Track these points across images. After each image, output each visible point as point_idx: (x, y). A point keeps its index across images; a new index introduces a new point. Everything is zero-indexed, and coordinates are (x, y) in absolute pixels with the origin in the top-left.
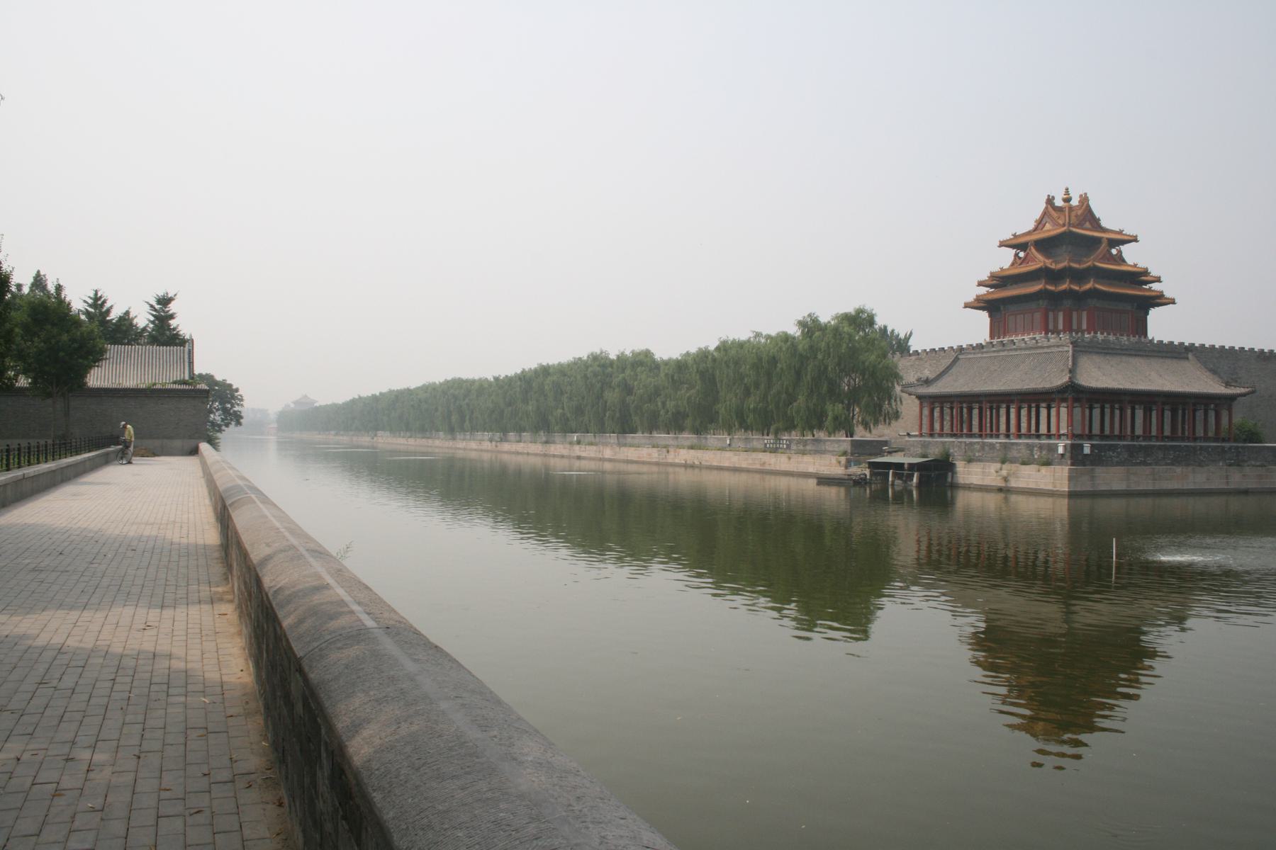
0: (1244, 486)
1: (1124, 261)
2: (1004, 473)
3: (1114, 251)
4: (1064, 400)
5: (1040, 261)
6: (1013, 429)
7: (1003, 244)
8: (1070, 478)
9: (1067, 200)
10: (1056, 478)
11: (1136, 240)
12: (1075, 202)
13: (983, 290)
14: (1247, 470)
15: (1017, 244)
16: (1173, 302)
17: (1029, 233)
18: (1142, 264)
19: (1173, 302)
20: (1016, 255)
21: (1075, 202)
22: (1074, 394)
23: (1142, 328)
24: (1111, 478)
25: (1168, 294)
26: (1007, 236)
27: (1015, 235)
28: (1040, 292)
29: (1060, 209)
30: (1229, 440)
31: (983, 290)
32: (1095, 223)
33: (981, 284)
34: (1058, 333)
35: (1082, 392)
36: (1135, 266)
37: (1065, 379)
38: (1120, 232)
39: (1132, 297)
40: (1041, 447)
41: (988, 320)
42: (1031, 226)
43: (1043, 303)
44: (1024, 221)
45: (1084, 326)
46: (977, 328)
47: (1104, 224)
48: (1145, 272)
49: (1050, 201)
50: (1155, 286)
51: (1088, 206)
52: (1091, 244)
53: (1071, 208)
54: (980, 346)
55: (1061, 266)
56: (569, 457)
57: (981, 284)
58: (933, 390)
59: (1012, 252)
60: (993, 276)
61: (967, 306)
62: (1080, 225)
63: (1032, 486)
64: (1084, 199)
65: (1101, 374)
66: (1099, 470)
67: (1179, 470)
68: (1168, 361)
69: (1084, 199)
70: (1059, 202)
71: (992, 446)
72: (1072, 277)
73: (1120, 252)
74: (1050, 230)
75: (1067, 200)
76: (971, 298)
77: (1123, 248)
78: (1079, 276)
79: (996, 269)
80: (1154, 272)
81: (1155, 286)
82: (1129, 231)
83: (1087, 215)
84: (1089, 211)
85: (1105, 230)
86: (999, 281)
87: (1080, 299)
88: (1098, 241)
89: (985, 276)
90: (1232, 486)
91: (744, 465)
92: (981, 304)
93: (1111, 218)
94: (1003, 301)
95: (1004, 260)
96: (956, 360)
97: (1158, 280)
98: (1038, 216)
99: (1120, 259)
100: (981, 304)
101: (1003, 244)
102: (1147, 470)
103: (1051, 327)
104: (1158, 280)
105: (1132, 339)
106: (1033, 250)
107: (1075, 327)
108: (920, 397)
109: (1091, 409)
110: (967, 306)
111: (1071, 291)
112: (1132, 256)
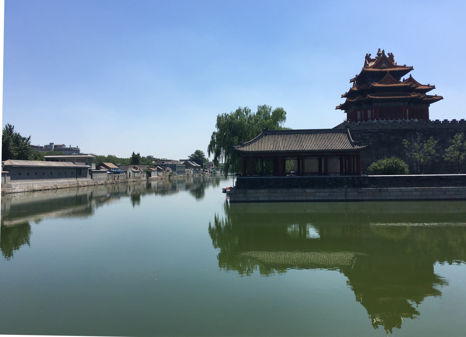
0: (360, 198)
11: (411, 69)
16: (441, 98)
19: (441, 98)
23: (426, 113)
38: (405, 66)
39: (419, 98)
66: (250, 191)
73: (410, 75)
97: (433, 87)
99: (411, 79)
104: (433, 87)
105: (390, 121)
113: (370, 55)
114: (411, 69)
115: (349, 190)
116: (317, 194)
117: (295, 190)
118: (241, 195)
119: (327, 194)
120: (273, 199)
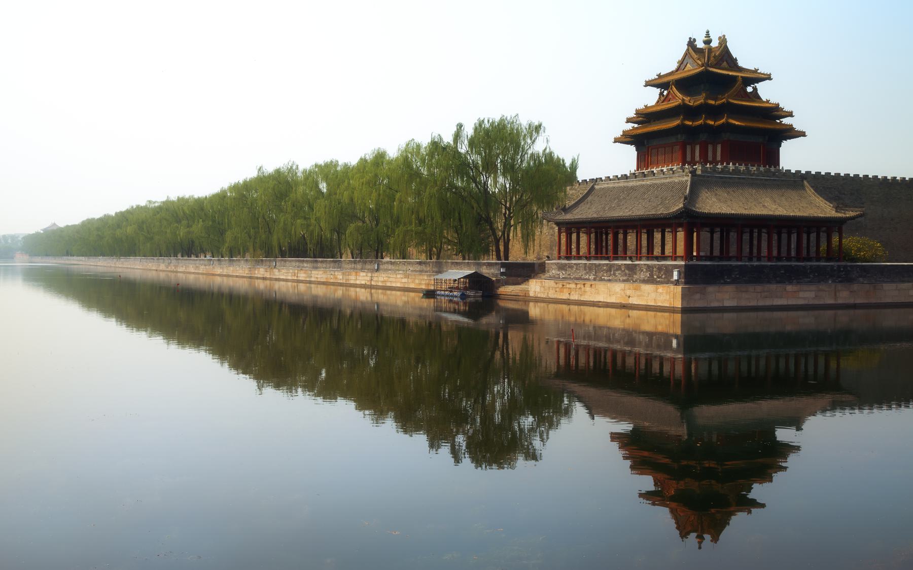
0: (852, 301)
1: (759, 98)
2: (628, 292)
3: (749, 89)
4: (680, 225)
5: (679, 98)
7: (649, 84)
8: (684, 296)
9: (708, 42)
10: (668, 295)
11: (768, 77)
12: (715, 44)
13: (630, 126)
14: (855, 287)
15: (661, 83)
16: (803, 134)
17: (672, 73)
18: (773, 100)
19: (803, 134)
20: (661, 94)
21: (715, 44)
22: (690, 220)
23: (773, 158)
24: (724, 296)
25: (798, 127)
27: (659, 76)
28: (678, 126)
30: (839, 261)
31: (630, 126)
32: (732, 63)
33: (629, 121)
34: (684, 164)
36: (768, 101)
37: (678, 206)
38: (756, 71)
40: (660, 268)
41: (636, 153)
42: (674, 67)
43: (681, 138)
45: (719, 158)
46: (625, 160)
47: (741, 64)
48: (777, 108)
49: (691, 43)
50: (786, 121)
51: (726, 47)
53: (710, 50)
54: (625, 177)
56: (271, 279)
57: (629, 121)
58: (569, 217)
59: (658, 91)
60: (638, 113)
62: (717, 65)
63: (652, 303)
64: (723, 41)
65: (714, 203)
66: (711, 289)
67: (789, 288)
68: (124, 218)
69: (723, 41)
70: (700, 45)
71: (619, 267)
72: (712, 112)
73: (755, 89)
74: (692, 69)
75: (708, 42)
76: (619, 134)
78: (715, 112)
80: (786, 106)
81: (786, 121)
83: (724, 56)
85: (741, 70)
86: (645, 117)
87: (714, 132)
88: (734, 78)
89: (632, 114)
90: (840, 301)
91: (412, 286)
92: (627, 138)
93: (747, 57)
94: (649, 136)
95: (651, 98)
96: (592, 188)
97: (790, 114)
98: (680, 58)
99: (755, 95)
100: (627, 138)
101: (649, 84)
102: (759, 288)
103: (689, 158)
104: (790, 114)
105: (762, 169)
106: (674, 89)
107: (710, 159)
108: (558, 224)
111: (706, 126)
112: (766, 92)
113: (695, 40)
114: (768, 77)
115: (839, 286)
116: (801, 294)
117: (773, 287)
118: (698, 296)
119: (812, 294)
120: (743, 303)
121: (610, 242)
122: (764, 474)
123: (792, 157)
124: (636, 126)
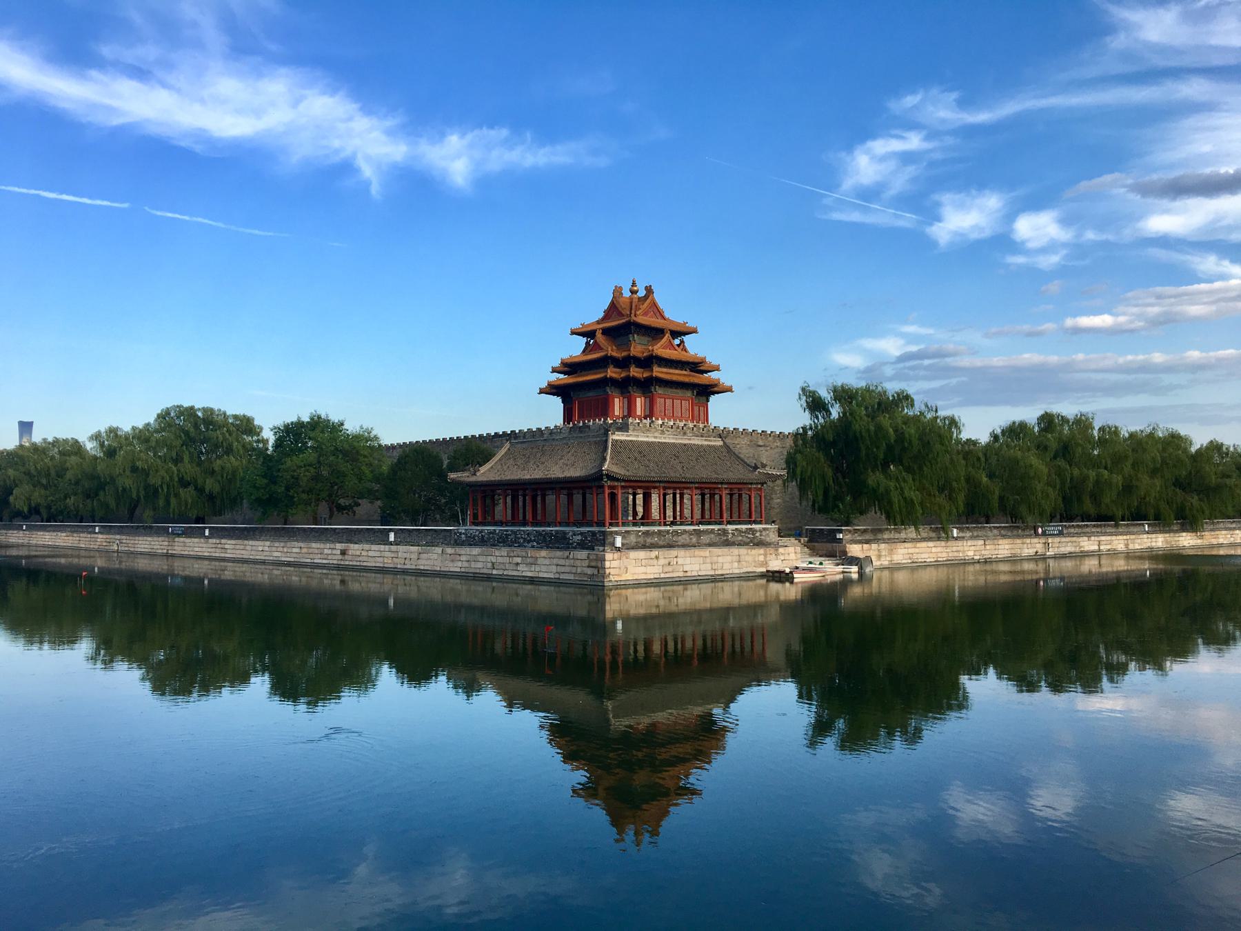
3: (677, 342)
6: (529, 516)
9: (633, 292)
11: (694, 331)
13: (555, 377)
15: (588, 334)
16: (729, 390)
17: (598, 322)
18: (701, 355)
19: (729, 390)
20: (587, 343)
21: (642, 293)
26: (577, 325)
29: (631, 299)
33: (554, 370)
35: (618, 480)
42: (601, 315)
44: (593, 312)
46: (551, 413)
47: (667, 315)
48: (703, 361)
49: (618, 291)
50: (713, 375)
52: (655, 333)
54: (551, 432)
55: (624, 354)
57: (554, 370)
60: (564, 364)
61: (542, 391)
64: (649, 290)
69: (649, 290)
70: (627, 294)
73: (682, 342)
76: (544, 385)
77: (686, 338)
79: (566, 356)
81: (713, 375)
82: (691, 324)
84: (654, 305)
86: (569, 367)
89: (557, 364)
92: (553, 390)
95: (575, 348)
97: (717, 369)
100: (553, 390)
101: (573, 333)
104: (717, 369)
109: (634, 495)
110: (542, 391)
112: (694, 347)
113: (621, 288)
121: (521, 504)
122: (702, 756)
123: (722, 413)
124: (562, 376)
